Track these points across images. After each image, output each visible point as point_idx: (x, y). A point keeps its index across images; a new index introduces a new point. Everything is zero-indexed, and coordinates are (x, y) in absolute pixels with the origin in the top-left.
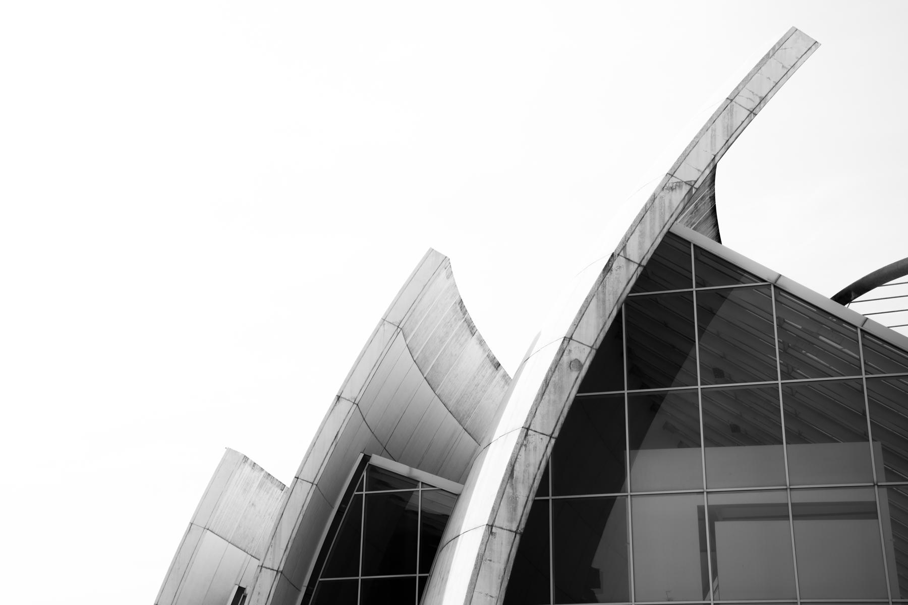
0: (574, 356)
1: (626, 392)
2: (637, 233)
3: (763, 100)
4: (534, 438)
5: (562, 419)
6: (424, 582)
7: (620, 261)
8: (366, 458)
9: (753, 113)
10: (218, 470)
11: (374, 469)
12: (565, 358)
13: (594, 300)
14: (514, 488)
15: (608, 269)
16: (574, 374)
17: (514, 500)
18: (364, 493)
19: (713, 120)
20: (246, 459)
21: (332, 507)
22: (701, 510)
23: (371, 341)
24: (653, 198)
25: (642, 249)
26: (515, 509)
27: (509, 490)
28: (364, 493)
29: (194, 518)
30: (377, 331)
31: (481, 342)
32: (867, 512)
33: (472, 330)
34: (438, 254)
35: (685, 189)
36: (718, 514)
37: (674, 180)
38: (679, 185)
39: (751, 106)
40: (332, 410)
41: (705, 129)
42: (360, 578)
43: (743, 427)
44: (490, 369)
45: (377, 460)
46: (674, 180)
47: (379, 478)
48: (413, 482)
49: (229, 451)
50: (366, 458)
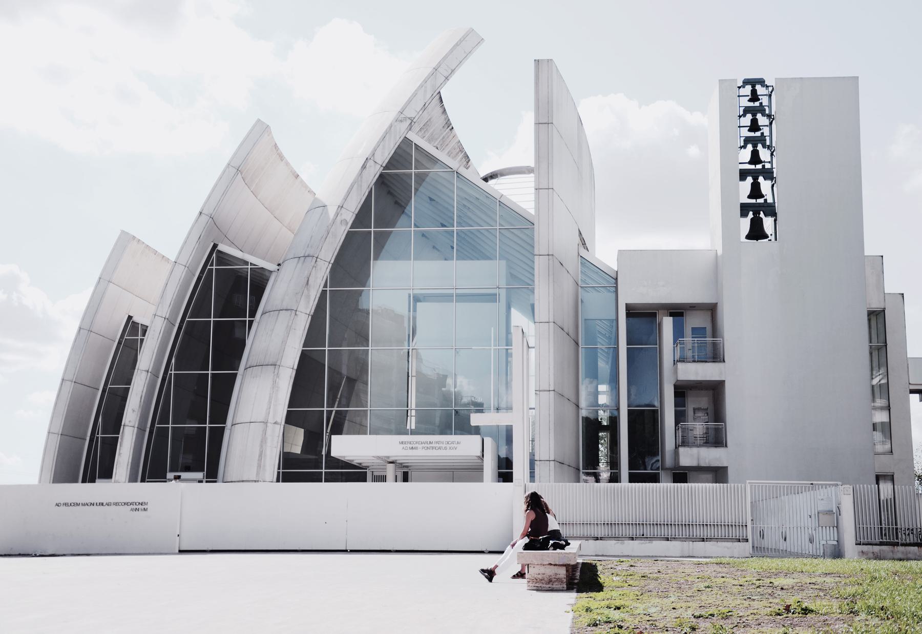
0: (344, 217)
1: (372, 230)
2: (381, 146)
3: (453, 71)
5: (336, 254)
6: (251, 323)
7: (371, 163)
8: (215, 246)
9: (447, 78)
10: (116, 244)
11: (219, 252)
12: (339, 218)
13: (356, 186)
14: (308, 290)
15: (364, 167)
16: (343, 228)
18: (214, 267)
19: (425, 81)
20: (134, 237)
21: (194, 275)
22: (410, 296)
23: (220, 178)
24: (391, 126)
25: (384, 157)
26: (309, 302)
27: (306, 291)
28: (214, 267)
29: (102, 274)
30: (224, 171)
31: (287, 164)
33: (281, 157)
34: (263, 123)
35: (409, 122)
36: (417, 299)
37: (402, 116)
39: (446, 74)
40: (197, 221)
41: (421, 86)
42: (212, 319)
43: (435, 247)
45: (221, 247)
46: (402, 116)
47: (223, 258)
48: (246, 263)
49: (123, 232)
50: (215, 246)
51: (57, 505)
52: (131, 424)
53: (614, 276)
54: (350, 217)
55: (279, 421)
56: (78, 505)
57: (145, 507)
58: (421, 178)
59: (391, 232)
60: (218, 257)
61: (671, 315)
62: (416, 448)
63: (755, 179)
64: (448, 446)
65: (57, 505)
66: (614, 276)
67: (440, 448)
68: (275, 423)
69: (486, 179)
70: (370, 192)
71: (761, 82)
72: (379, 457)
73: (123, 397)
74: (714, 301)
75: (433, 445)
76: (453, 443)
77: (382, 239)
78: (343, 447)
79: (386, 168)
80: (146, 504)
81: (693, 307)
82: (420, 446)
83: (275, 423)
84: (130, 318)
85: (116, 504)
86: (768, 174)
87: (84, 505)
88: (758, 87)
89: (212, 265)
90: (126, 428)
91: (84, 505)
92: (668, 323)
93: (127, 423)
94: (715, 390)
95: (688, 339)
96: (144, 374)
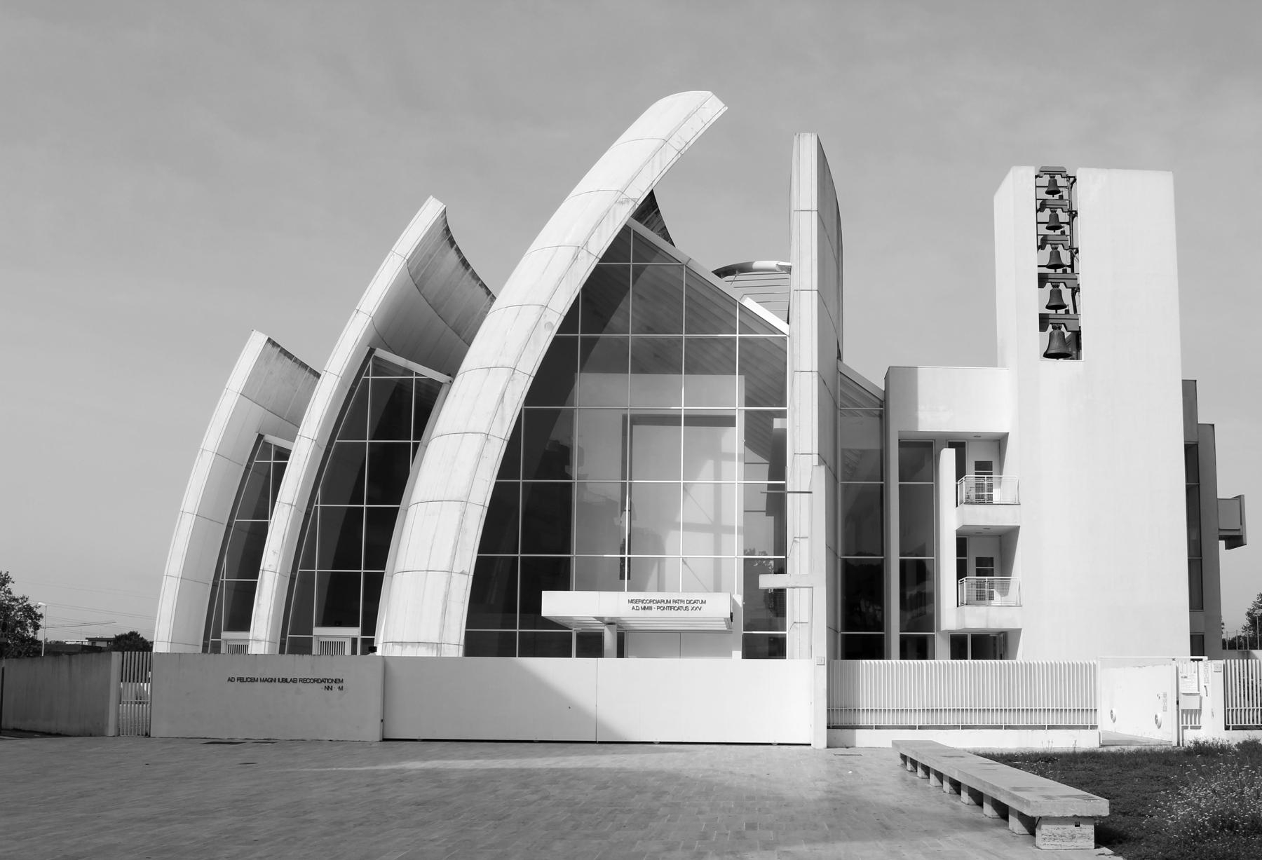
0: (548, 320)
4: (518, 376)
6: (416, 446)
7: (583, 253)
8: (371, 351)
11: (376, 358)
17: (503, 419)
22: (625, 418)
31: (458, 250)
32: (729, 421)
35: (631, 204)
38: (627, 200)
44: (462, 269)
45: (380, 353)
48: (411, 373)
52: (273, 569)
53: (881, 396)
54: (557, 321)
56: (253, 680)
58: (638, 271)
59: (597, 339)
60: (374, 364)
61: (951, 445)
62: (650, 608)
63: (1056, 286)
64: (690, 606)
66: (881, 396)
69: (722, 273)
71: (1061, 172)
72: (598, 618)
73: (258, 536)
75: (672, 605)
77: (589, 344)
78: (554, 604)
79: (601, 260)
81: (978, 438)
84: (260, 437)
85: (304, 681)
88: (1058, 177)
89: (367, 374)
92: (948, 458)
93: (267, 567)
94: (1005, 540)
95: (971, 475)
96: (287, 508)
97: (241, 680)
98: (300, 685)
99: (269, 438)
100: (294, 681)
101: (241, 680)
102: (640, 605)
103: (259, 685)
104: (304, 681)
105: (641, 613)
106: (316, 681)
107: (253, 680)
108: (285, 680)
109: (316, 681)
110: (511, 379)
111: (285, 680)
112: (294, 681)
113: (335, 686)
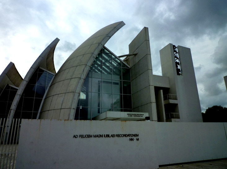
4: (87, 66)
8: (39, 67)
17: (84, 75)
50: (39, 67)
51: (74, 136)
52: (14, 109)
55: (75, 108)
56: (89, 136)
57: (137, 137)
62: (132, 116)
65: (74, 136)
67: (138, 116)
68: (73, 109)
70: (38, 79)
74: (169, 87)
75: (137, 115)
76: (142, 115)
80: (137, 135)
82: (133, 115)
83: (73, 109)
85: (118, 136)
86: (177, 63)
87: (95, 136)
90: (12, 111)
91: (95, 136)
93: (12, 109)
96: (19, 96)
97: (82, 136)
98: (116, 138)
99: (10, 85)
100: (113, 136)
101: (82, 136)
102: (130, 115)
103: (93, 138)
104: (118, 136)
105: (130, 117)
106: (125, 135)
107: (89, 136)
108: (108, 136)
109: (125, 135)
110: (86, 67)
111: (108, 136)
112: (113, 136)
113: (135, 138)
